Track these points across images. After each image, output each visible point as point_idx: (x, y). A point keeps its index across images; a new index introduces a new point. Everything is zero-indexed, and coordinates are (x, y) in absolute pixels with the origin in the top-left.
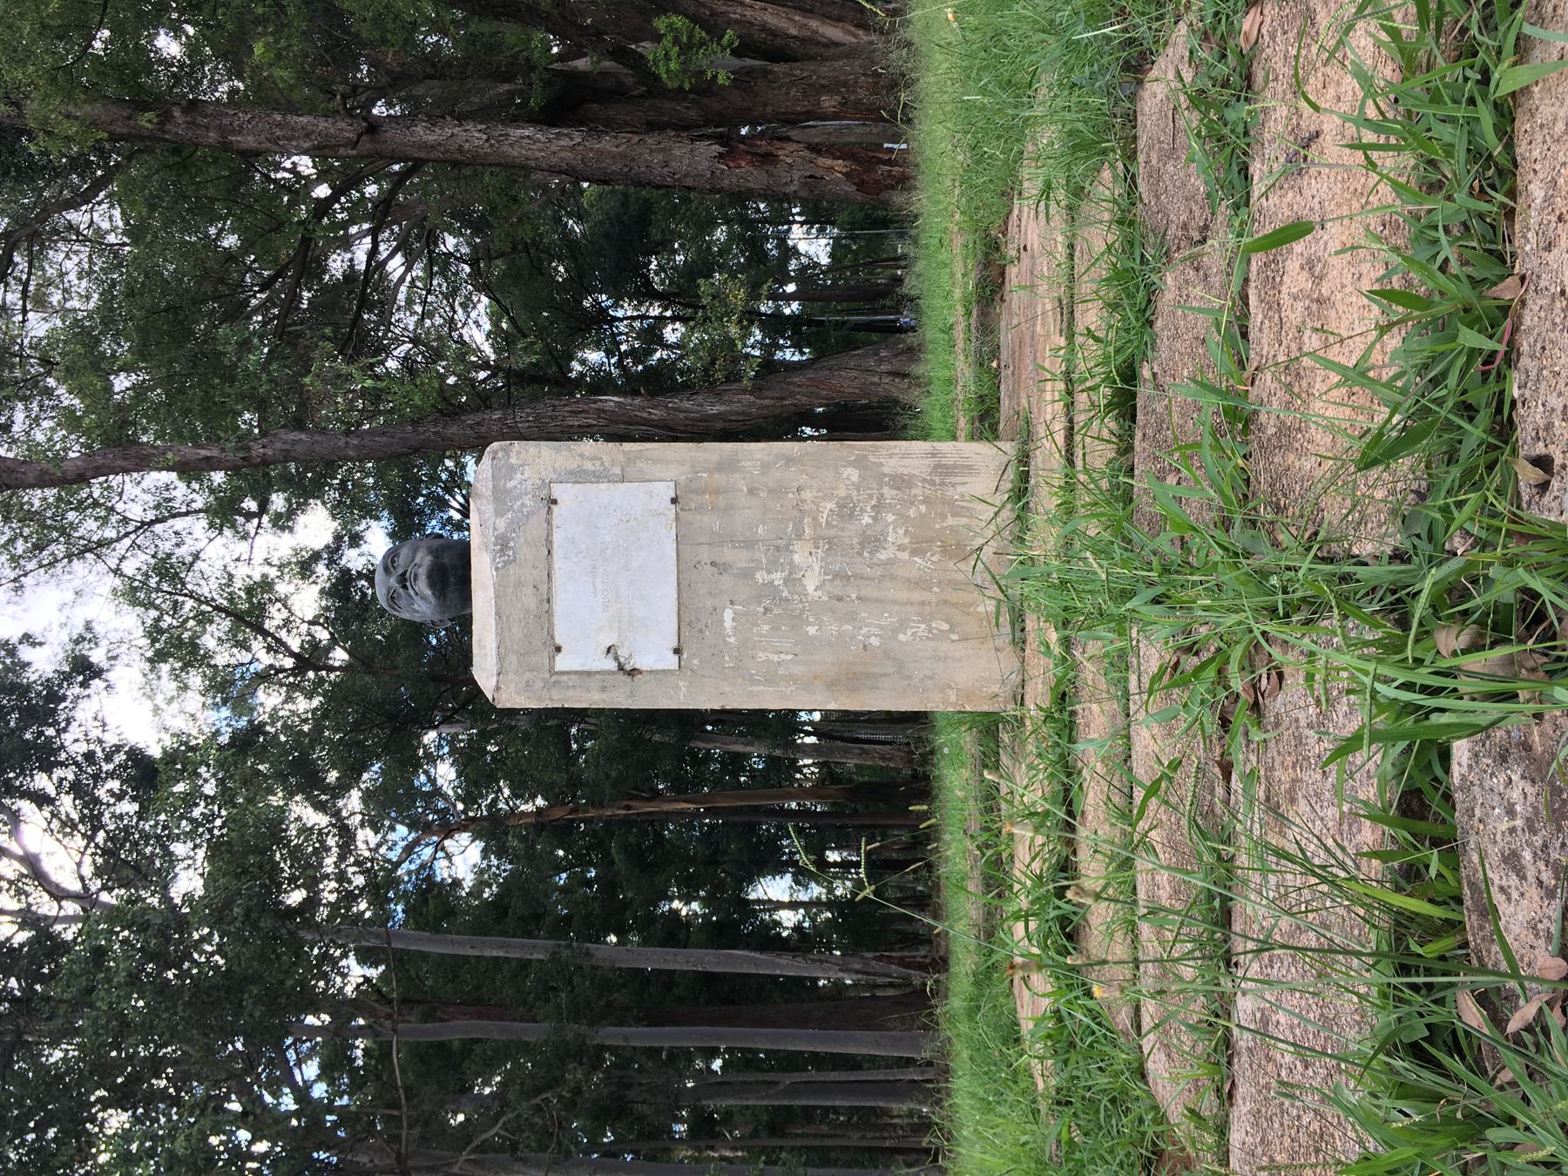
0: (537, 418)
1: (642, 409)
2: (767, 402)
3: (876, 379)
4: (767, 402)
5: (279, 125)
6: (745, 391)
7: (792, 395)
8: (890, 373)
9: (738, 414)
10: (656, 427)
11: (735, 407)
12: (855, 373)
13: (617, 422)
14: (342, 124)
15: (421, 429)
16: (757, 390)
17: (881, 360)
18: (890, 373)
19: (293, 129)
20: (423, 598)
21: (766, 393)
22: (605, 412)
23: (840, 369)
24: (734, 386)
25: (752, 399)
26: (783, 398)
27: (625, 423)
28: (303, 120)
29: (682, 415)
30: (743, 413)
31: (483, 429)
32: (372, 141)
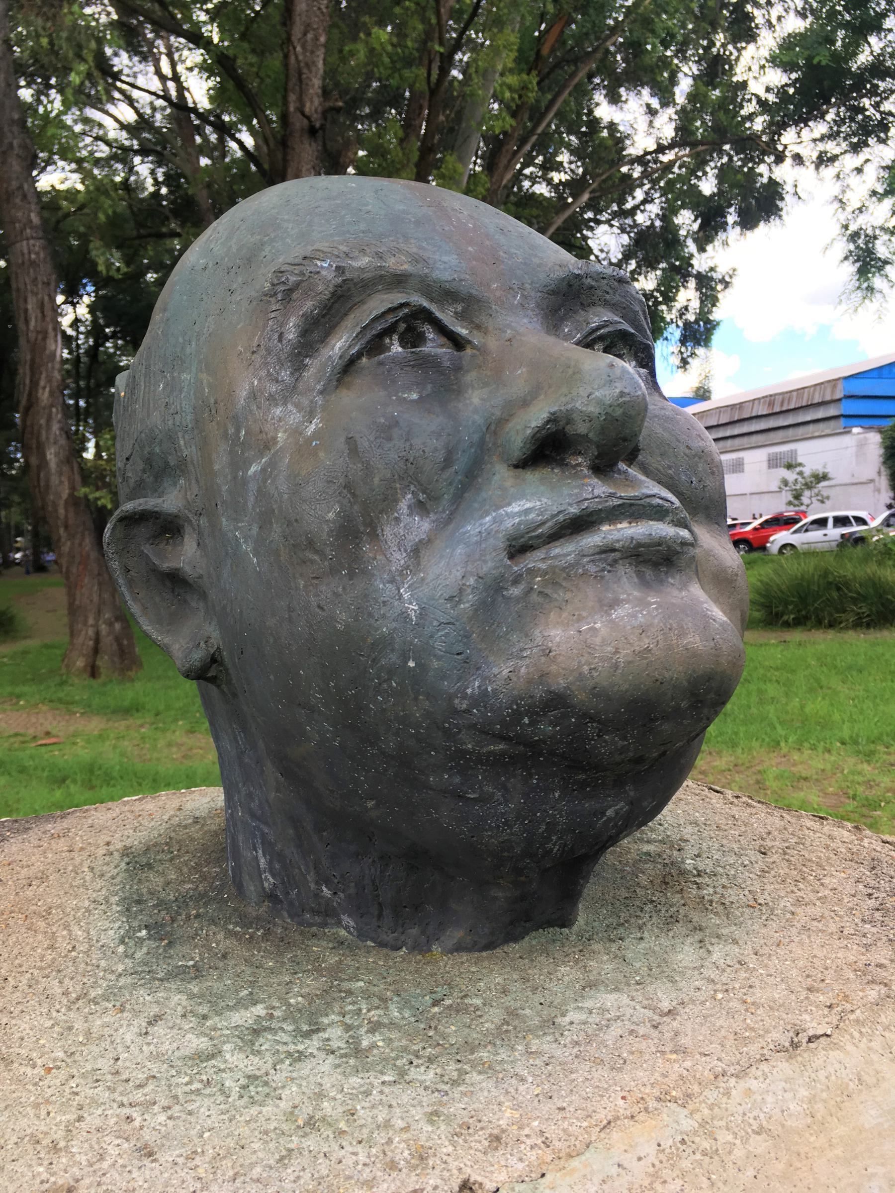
0: (32, 263)
1: (49, 380)
2: (61, 511)
3: (91, 621)
4: (61, 511)
5: (316, 39)
6: (73, 488)
7: (71, 537)
8: (98, 634)
9: (48, 480)
10: (30, 395)
11: (54, 480)
12: (96, 598)
13: (33, 351)
14: (317, 101)
15: (15, 129)
16: (74, 501)
17: (110, 624)
18: (98, 634)
19: (312, 52)
20: (497, 605)
21: (71, 509)
22: (45, 338)
23: (100, 584)
24: (77, 478)
25: (65, 495)
26: (66, 527)
27: (33, 361)
28: (320, 64)
29: (43, 422)
30: (48, 486)
31: (18, 201)
32: (303, 129)
